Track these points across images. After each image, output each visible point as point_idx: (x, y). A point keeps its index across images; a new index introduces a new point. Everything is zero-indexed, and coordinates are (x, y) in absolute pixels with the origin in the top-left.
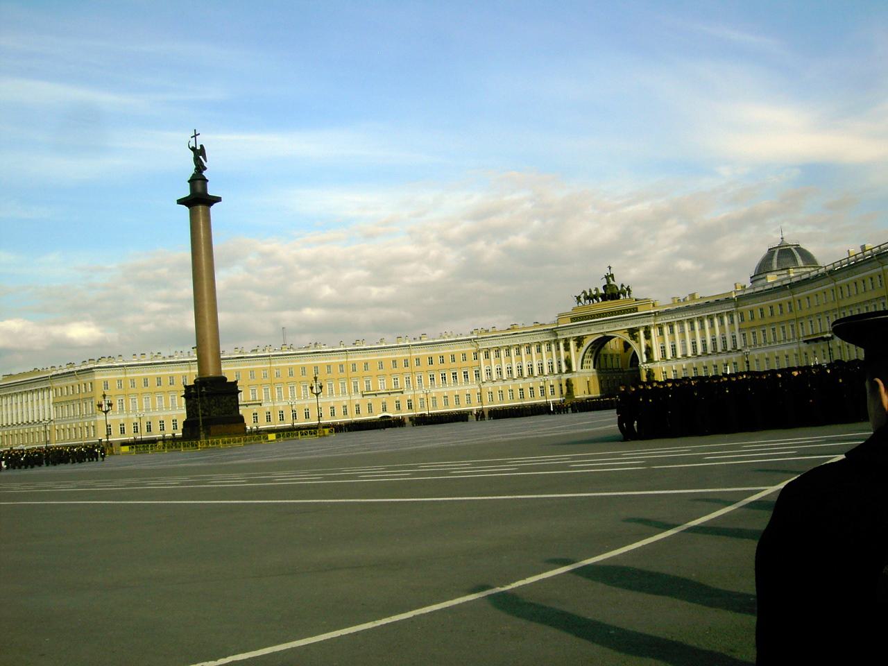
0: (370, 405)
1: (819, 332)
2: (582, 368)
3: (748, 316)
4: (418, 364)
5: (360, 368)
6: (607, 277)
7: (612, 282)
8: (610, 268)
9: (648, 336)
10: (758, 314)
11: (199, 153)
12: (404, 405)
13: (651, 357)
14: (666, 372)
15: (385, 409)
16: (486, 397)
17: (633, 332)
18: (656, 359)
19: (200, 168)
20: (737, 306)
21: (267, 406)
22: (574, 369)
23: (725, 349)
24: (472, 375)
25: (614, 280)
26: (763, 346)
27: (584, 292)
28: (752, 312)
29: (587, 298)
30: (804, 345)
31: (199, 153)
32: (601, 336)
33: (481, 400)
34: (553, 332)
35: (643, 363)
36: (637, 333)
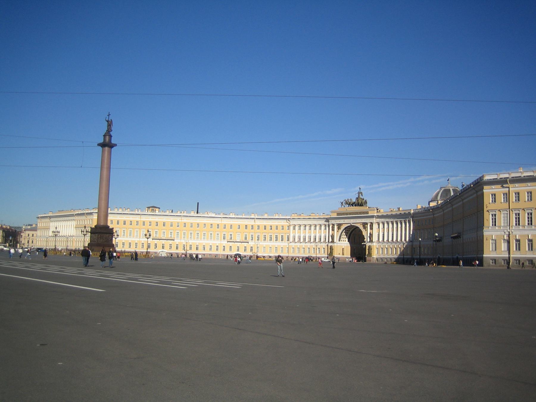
0: (231, 247)
2: (339, 241)
4: (259, 229)
5: (228, 227)
6: (359, 193)
7: (361, 197)
9: (371, 228)
11: (110, 124)
12: (249, 249)
15: (238, 250)
16: (291, 250)
17: (365, 225)
18: (374, 241)
19: (109, 131)
21: (177, 241)
24: (285, 238)
25: (362, 195)
29: (346, 203)
31: (110, 124)
32: (349, 225)
33: (288, 252)
34: (327, 220)
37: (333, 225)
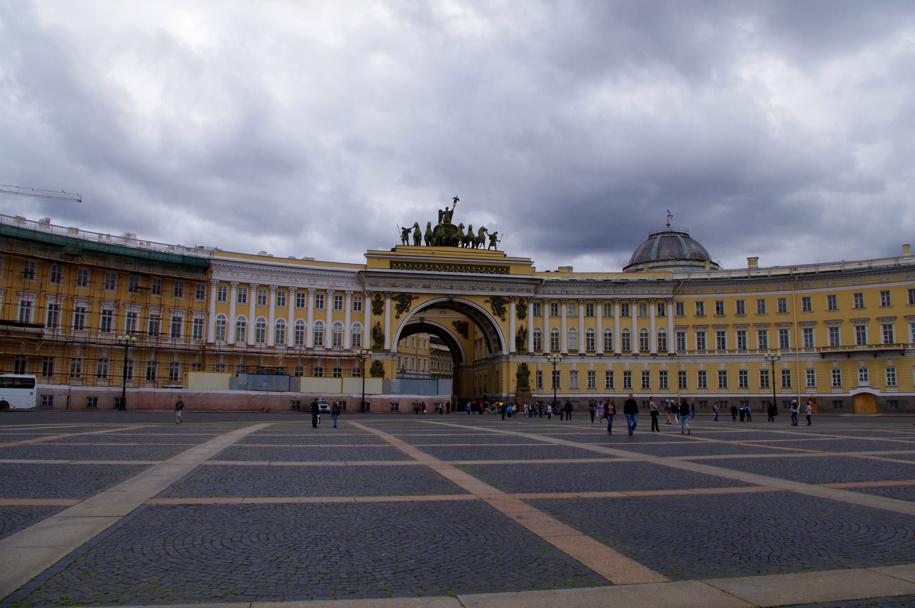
1: (829, 345)
3: (690, 309)
8: (456, 200)
9: (521, 315)
10: (710, 309)
13: (525, 347)
14: (540, 373)
17: (499, 304)
20: (675, 293)
22: (387, 347)
23: (644, 349)
26: (716, 353)
27: (416, 226)
28: (700, 304)
30: (811, 362)
35: (511, 353)
37: (378, 294)
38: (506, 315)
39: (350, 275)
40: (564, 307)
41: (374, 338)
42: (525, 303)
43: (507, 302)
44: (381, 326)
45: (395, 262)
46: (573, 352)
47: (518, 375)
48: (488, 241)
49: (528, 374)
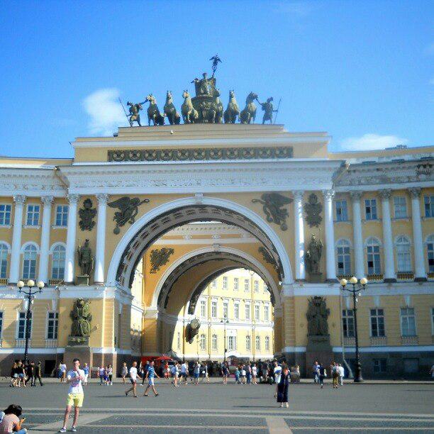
6: (199, 85)
8: (216, 61)
13: (321, 270)
22: (100, 276)
35: (297, 281)
36: (285, 207)
38: (288, 220)
39: (46, 173)
40: (386, 205)
41: (80, 264)
42: (319, 201)
43: (290, 200)
44: (91, 246)
45: (115, 152)
46: (405, 275)
47: (310, 317)
48: (260, 114)
49: (326, 314)
